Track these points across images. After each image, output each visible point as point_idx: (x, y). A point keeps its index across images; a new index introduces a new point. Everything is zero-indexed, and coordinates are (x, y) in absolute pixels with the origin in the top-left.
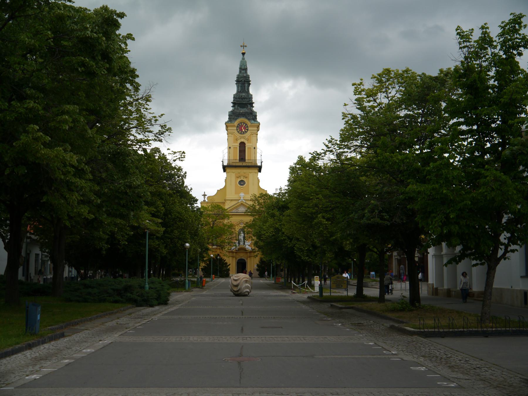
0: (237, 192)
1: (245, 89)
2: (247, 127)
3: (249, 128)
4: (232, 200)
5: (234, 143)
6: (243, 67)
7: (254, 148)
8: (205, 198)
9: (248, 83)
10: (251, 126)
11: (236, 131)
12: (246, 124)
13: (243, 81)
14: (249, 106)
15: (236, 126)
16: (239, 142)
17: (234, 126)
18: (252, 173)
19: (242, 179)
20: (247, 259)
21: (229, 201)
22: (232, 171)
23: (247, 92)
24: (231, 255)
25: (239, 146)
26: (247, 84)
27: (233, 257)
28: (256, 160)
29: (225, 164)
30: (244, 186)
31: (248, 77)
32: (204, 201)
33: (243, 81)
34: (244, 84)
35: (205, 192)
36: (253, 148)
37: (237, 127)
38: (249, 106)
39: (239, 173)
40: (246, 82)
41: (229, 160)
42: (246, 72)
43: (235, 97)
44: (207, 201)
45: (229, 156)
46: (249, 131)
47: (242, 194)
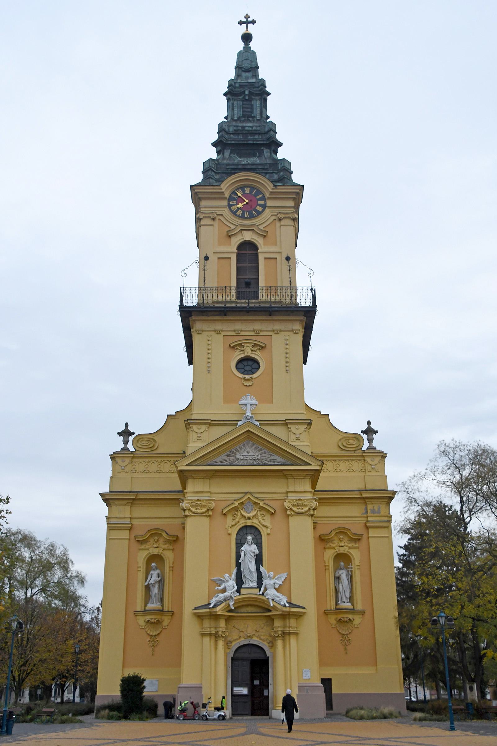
0: (230, 397)
1: (252, 112)
2: (263, 198)
3: (269, 203)
4: (211, 424)
5: (220, 244)
6: (246, 65)
7: (288, 259)
8: (126, 442)
9: (260, 99)
10: (275, 196)
12: (259, 192)
13: (247, 92)
14: (265, 151)
15: (227, 195)
16: (236, 241)
17: (220, 196)
19: (248, 352)
20: (272, 645)
21: (204, 427)
22: (213, 326)
23: (258, 120)
24: (208, 631)
25: (238, 256)
26: (258, 102)
27: (216, 636)
28: (293, 288)
29: (192, 300)
30: (255, 376)
31: (260, 84)
32: (125, 449)
33: (247, 92)
34: (250, 100)
35: (127, 425)
36: (281, 259)
37: (230, 199)
38: (265, 151)
39: (238, 334)
40: (257, 95)
41: (202, 289)
42: (256, 75)
43: (222, 129)
44: (132, 449)
45: (203, 279)
46: (267, 210)
47: (249, 400)
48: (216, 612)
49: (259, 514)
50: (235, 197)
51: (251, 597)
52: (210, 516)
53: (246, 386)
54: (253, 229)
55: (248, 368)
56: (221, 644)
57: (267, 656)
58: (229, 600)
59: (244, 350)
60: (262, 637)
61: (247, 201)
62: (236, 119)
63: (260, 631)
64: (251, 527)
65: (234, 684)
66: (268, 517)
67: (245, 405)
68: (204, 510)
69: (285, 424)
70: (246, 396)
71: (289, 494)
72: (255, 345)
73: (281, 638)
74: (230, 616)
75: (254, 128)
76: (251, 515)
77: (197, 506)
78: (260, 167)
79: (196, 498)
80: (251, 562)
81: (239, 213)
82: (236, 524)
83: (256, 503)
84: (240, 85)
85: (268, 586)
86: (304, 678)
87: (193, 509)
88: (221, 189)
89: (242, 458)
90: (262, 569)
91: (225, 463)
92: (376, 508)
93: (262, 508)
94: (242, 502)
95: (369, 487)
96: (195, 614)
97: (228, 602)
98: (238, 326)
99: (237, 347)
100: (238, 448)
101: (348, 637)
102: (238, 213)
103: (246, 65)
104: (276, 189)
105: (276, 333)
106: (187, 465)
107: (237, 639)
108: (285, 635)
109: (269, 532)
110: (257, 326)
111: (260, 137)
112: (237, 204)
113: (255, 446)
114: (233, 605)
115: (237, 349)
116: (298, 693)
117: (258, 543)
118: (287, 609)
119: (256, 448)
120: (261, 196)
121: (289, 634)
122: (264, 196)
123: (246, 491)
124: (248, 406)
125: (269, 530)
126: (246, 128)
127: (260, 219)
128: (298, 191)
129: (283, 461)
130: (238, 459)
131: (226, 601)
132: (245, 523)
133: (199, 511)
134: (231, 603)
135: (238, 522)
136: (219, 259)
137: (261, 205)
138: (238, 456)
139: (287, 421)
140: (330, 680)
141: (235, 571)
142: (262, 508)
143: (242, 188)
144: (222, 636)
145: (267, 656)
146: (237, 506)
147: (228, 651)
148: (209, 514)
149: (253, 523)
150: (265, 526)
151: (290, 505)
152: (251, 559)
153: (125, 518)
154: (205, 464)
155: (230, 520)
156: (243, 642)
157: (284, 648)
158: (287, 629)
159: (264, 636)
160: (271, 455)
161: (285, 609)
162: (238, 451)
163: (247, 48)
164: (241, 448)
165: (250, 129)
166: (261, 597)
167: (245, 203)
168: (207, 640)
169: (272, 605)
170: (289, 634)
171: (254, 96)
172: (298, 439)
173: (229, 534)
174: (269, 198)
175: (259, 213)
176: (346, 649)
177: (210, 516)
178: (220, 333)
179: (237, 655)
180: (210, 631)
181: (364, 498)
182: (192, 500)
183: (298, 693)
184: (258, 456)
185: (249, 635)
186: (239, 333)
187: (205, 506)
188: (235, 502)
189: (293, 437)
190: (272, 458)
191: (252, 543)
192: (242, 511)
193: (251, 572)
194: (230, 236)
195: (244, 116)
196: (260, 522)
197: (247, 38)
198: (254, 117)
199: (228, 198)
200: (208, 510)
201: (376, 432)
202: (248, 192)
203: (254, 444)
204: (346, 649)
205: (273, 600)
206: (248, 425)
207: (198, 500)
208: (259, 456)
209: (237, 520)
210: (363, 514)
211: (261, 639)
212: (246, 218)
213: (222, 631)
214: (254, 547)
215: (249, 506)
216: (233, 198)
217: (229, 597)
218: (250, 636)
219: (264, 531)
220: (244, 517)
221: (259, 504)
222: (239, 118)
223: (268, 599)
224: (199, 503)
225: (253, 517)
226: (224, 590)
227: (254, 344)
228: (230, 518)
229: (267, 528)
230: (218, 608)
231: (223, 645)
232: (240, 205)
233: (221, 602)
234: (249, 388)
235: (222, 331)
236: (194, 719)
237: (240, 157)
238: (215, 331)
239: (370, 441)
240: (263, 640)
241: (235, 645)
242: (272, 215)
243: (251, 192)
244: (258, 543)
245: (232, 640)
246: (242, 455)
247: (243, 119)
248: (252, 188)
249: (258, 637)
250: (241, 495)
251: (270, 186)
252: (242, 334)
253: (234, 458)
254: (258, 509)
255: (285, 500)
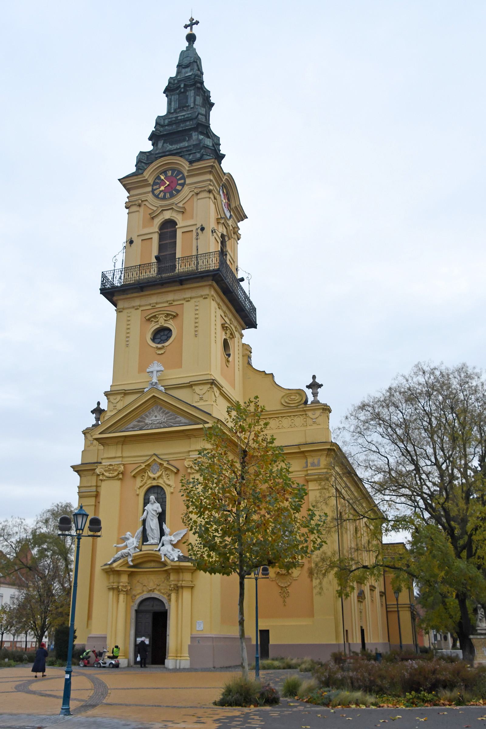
1: (187, 102)
2: (183, 178)
5: (144, 227)
11: (150, 195)
12: (180, 172)
13: (182, 86)
15: (151, 181)
16: (158, 221)
18: (193, 301)
19: (162, 322)
21: (119, 397)
23: (191, 108)
30: (166, 344)
34: (185, 92)
37: (155, 183)
38: (194, 134)
40: (191, 85)
46: (186, 188)
47: (156, 367)
48: (113, 568)
49: (164, 474)
50: (159, 181)
51: (151, 554)
52: (120, 479)
53: (159, 354)
54: (173, 208)
55: (164, 338)
56: (122, 597)
57: (166, 608)
58: (127, 556)
59: (157, 322)
60: (163, 591)
61: (168, 183)
62: (172, 111)
63: (161, 585)
64: (158, 487)
65: (138, 634)
66: (172, 477)
67: (152, 372)
68: (116, 473)
69: (190, 386)
70: (153, 364)
71: (191, 453)
72: (168, 315)
73: (174, 591)
74: (132, 572)
75: (186, 116)
76: (156, 476)
77: (110, 471)
78: (185, 150)
79: (109, 464)
80: (152, 520)
81: (162, 195)
82: (143, 485)
83: (161, 464)
84: (178, 81)
85: (165, 543)
86: (198, 629)
87: (107, 474)
88: (144, 177)
89: (150, 422)
90: (164, 526)
91: (136, 429)
92: (316, 461)
93: (166, 469)
94: (148, 464)
95: (309, 440)
96: (103, 570)
97: (126, 558)
98: (153, 300)
99: (152, 319)
100: (147, 413)
101: (287, 590)
102: (160, 196)
103: (186, 62)
104: (192, 166)
105: (187, 301)
106: (100, 434)
107: (140, 593)
108: (178, 589)
109: (172, 491)
110: (170, 297)
111: (191, 123)
112: (160, 188)
113: (162, 410)
114: (132, 561)
115: (152, 321)
116: (189, 643)
117: (162, 501)
118: (177, 564)
119: (163, 412)
120: (181, 175)
121: (182, 587)
122: (183, 175)
123: (151, 453)
124: (155, 373)
125: (172, 488)
126: (179, 118)
127: (179, 197)
128: (212, 164)
129: (187, 421)
130: (147, 424)
131: (124, 557)
132: (151, 483)
133: (111, 475)
134: (130, 559)
135: (146, 483)
136: (143, 241)
137: (180, 185)
138: (147, 421)
139: (191, 383)
140: (267, 631)
141: (141, 528)
142: (166, 469)
143: (164, 172)
144: (122, 590)
145: (166, 608)
146: (144, 468)
147: (132, 604)
148: (121, 476)
149: (158, 483)
150: (169, 485)
151: (191, 464)
152: (153, 517)
153: (91, 486)
154: (119, 431)
155: (138, 482)
156: (146, 595)
157: (177, 601)
158: (180, 583)
159: (164, 589)
160: (176, 418)
161: (173, 564)
162: (147, 416)
163: (190, 47)
164: (150, 413)
165: (183, 117)
166: (157, 553)
167: (167, 185)
168: (111, 593)
169: (163, 560)
170: (182, 587)
171: (189, 87)
172: (201, 399)
173: (138, 495)
174: (189, 176)
175: (178, 192)
176: (284, 601)
177: (120, 479)
178: (138, 309)
179: (142, 608)
180: (112, 586)
181: (303, 452)
182: (106, 465)
183: (189, 643)
184: (164, 419)
185: (150, 589)
186: (154, 306)
187: (116, 470)
188: (142, 464)
189: (197, 398)
190: (177, 419)
191: (155, 502)
192: (149, 472)
193: (152, 529)
194: (153, 218)
195: (179, 108)
196: (164, 482)
197: (191, 38)
198: (189, 106)
199: (152, 183)
200: (119, 474)
201: (320, 386)
202: (170, 174)
203: (161, 409)
204: (284, 601)
205: (165, 555)
206: (153, 390)
207: (110, 465)
208: (166, 419)
209: (144, 481)
210: (304, 468)
211: (161, 593)
212: (167, 199)
213: (123, 586)
214: (158, 505)
215: (155, 467)
216: (157, 182)
217: (126, 553)
218: (151, 590)
219: (168, 490)
220: (150, 477)
221: (163, 464)
222: (175, 110)
223: (161, 554)
224: (111, 467)
225: (158, 477)
226: (126, 546)
227: (167, 314)
228: (139, 479)
229: (171, 487)
230: (115, 565)
231: (124, 599)
232: (162, 188)
233: (119, 559)
234: (164, 355)
235: (140, 306)
236: (94, 667)
237: (171, 145)
238: (133, 307)
239: (315, 394)
240: (163, 594)
241: (139, 599)
242: (191, 191)
243: (172, 174)
244: (162, 501)
245: (136, 594)
246: (150, 419)
247: (178, 110)
248: (173, 170)
249: (159, 590)
250: (148, 458)
251: (186, 165)
252: (158, 306)
253: (143, 423)
254: (163, 470)
255: (185, 459)
